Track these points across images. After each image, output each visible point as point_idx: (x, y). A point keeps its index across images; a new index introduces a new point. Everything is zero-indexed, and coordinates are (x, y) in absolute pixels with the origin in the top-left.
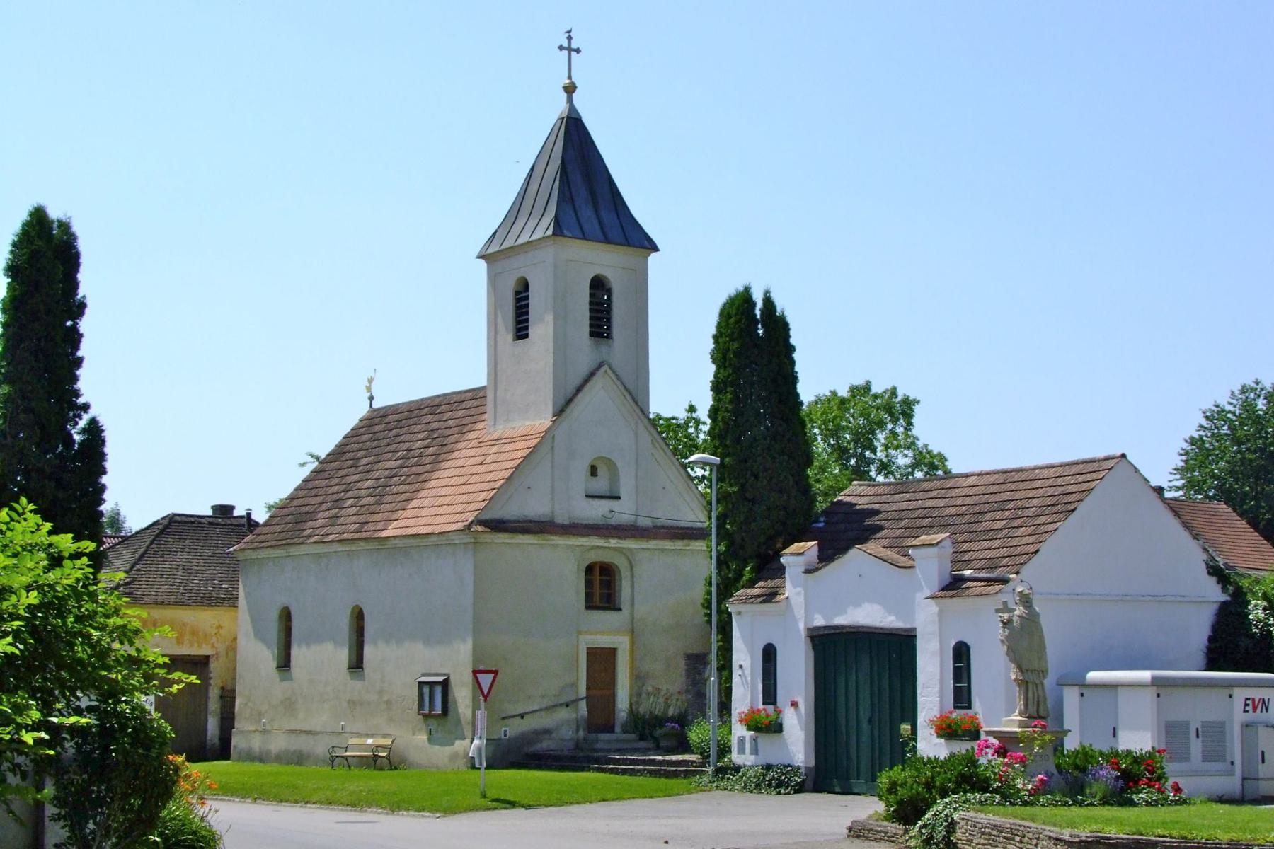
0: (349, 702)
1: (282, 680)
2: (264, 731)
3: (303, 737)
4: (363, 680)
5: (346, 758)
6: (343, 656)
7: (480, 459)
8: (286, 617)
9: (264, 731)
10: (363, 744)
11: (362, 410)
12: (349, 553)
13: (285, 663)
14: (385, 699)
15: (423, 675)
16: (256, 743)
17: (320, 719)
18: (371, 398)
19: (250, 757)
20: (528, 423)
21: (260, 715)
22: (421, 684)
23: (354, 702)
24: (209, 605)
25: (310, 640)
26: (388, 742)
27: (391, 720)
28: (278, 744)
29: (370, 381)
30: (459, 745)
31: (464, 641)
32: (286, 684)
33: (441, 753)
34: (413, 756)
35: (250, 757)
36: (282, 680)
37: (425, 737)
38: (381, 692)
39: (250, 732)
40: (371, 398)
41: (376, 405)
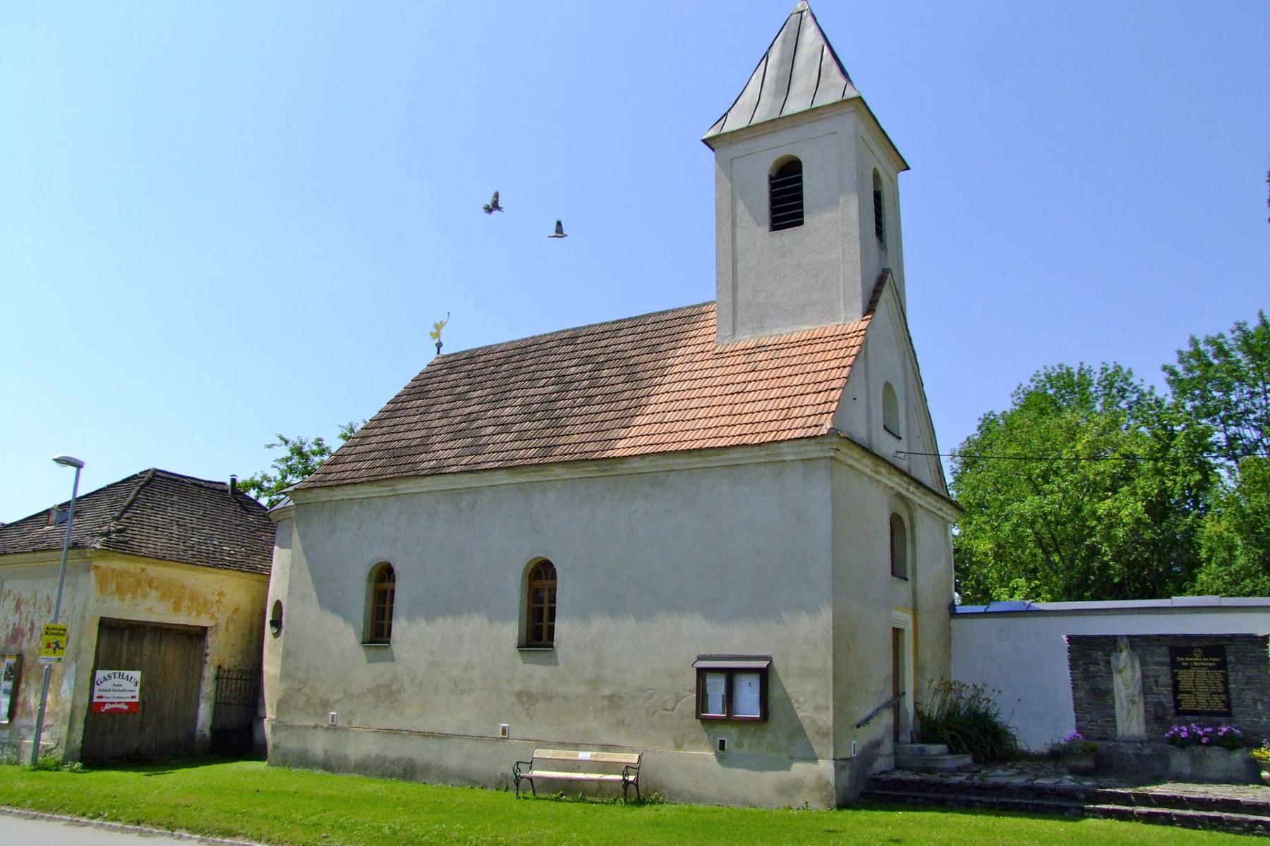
0: (519, 695)
1: (370, 661)
2: (333, 728)
3: (418, 741)
4: (557, 664)
5: (530, 779)
6: (511, 631)
7: (750, 367)
8: (384, 576)
9: (333, 728)
10: (587, 761)
11: (430, 356)
12: (521, 487)
13: (378, 632)
14: (607, 691)
15: (700, 658)
16: (291, 743)
17: (454, 716)
18: (439, 345)
19: (304, 761)
20: (807, 327)
21: (326, 705)
22: (702, 672)
23: (530, 696)
24: (215, 566)
25: (431, 609)
26: (633, 758)
27: (621, 723)
28: (362, 746)
29: (439, 327)
30: (799, 769)
31: (813, 611)
32: (380, 666)
33: (755, 783)
34: (676, 780)
35: (304, 761)
36: (370, 661)
37: (710, 754)
38: (595, 683)
39: (307, 727)
40: (439, 345)
41: (444, 351)
